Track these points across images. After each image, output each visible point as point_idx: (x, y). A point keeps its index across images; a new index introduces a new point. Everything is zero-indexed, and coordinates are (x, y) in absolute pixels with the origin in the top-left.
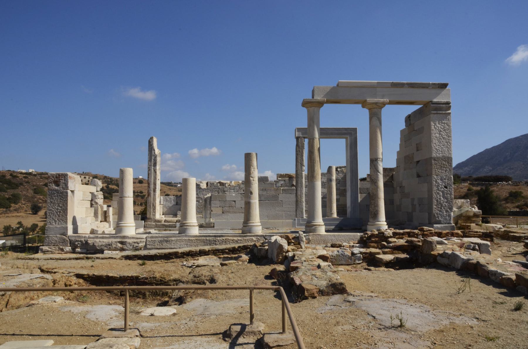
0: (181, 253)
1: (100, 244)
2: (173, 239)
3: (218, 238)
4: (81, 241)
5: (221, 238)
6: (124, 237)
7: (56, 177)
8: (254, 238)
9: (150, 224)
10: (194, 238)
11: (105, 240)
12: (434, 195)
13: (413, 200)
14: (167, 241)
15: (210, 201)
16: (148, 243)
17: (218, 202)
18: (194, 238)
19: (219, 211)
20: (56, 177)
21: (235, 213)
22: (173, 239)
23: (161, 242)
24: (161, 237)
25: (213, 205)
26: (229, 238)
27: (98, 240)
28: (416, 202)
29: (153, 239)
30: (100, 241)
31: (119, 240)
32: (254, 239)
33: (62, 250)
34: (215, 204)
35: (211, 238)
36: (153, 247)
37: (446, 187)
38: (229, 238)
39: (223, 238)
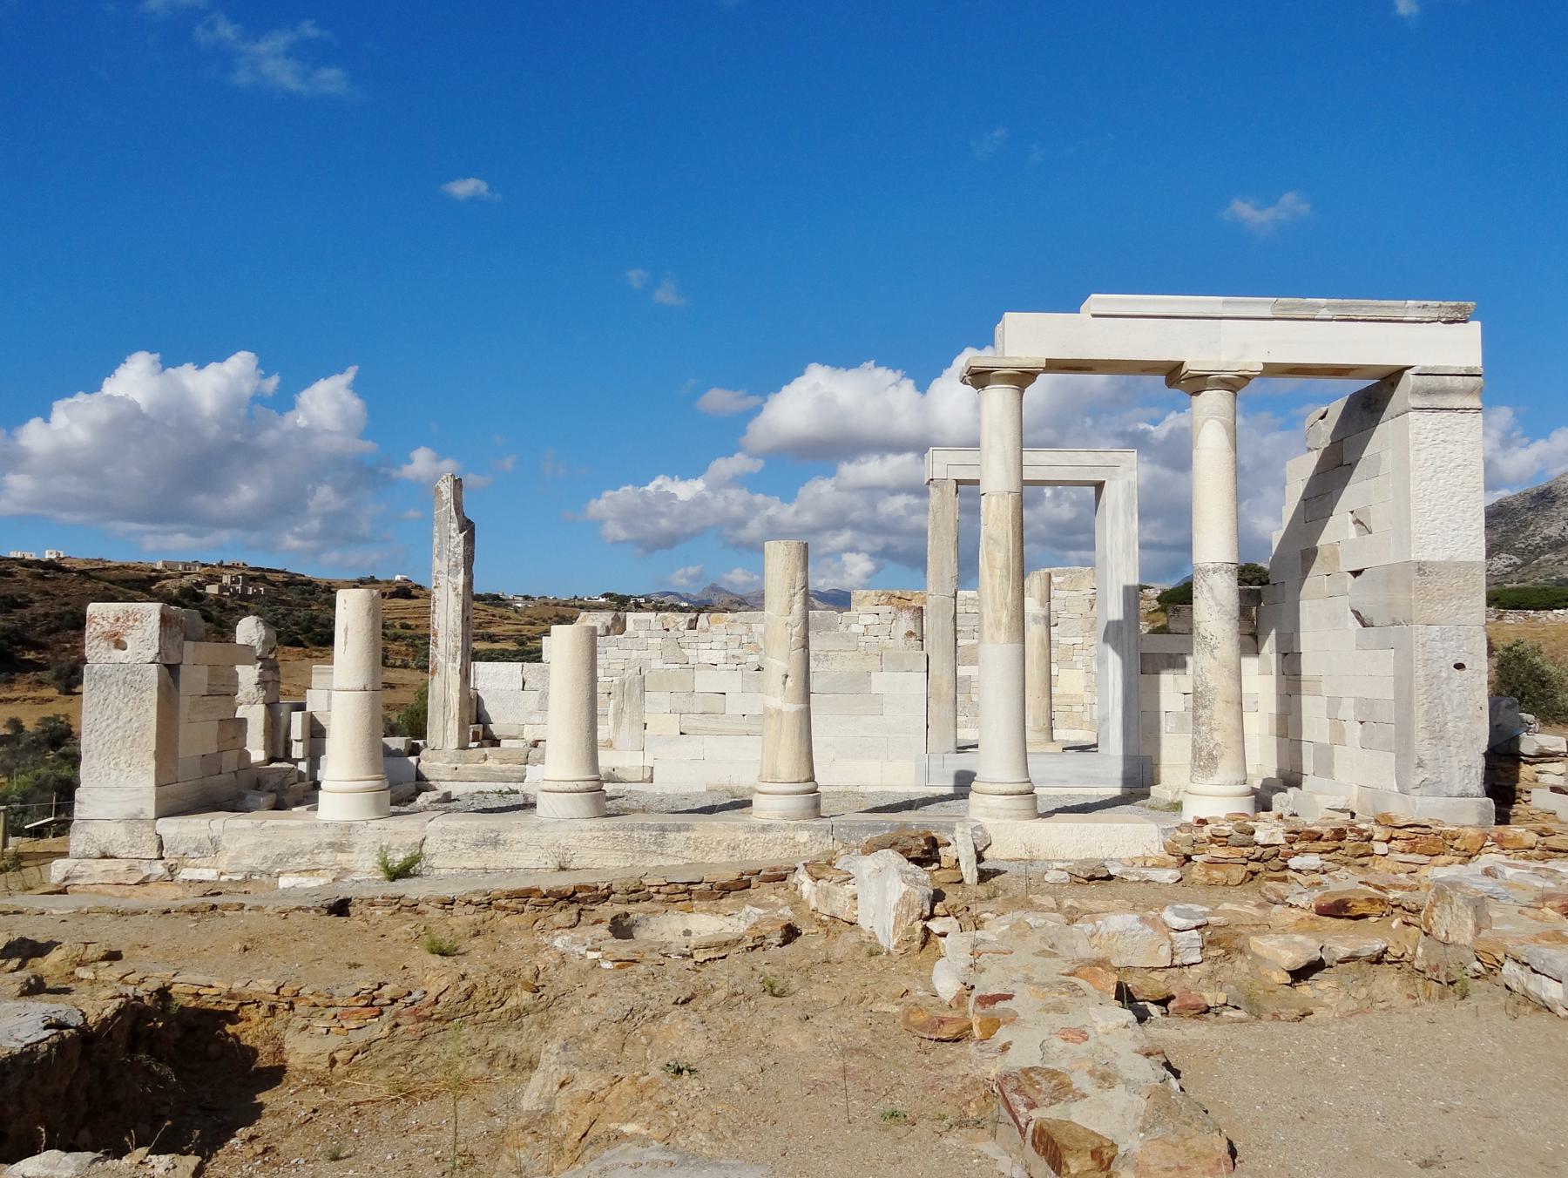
0: (550, 893)
2: (516, 836)
13: (1334, 703)
14: (495, 843)
19: (672, 725)
25: (648, 708)
28: (1348, 711)
37: (1459, 666)
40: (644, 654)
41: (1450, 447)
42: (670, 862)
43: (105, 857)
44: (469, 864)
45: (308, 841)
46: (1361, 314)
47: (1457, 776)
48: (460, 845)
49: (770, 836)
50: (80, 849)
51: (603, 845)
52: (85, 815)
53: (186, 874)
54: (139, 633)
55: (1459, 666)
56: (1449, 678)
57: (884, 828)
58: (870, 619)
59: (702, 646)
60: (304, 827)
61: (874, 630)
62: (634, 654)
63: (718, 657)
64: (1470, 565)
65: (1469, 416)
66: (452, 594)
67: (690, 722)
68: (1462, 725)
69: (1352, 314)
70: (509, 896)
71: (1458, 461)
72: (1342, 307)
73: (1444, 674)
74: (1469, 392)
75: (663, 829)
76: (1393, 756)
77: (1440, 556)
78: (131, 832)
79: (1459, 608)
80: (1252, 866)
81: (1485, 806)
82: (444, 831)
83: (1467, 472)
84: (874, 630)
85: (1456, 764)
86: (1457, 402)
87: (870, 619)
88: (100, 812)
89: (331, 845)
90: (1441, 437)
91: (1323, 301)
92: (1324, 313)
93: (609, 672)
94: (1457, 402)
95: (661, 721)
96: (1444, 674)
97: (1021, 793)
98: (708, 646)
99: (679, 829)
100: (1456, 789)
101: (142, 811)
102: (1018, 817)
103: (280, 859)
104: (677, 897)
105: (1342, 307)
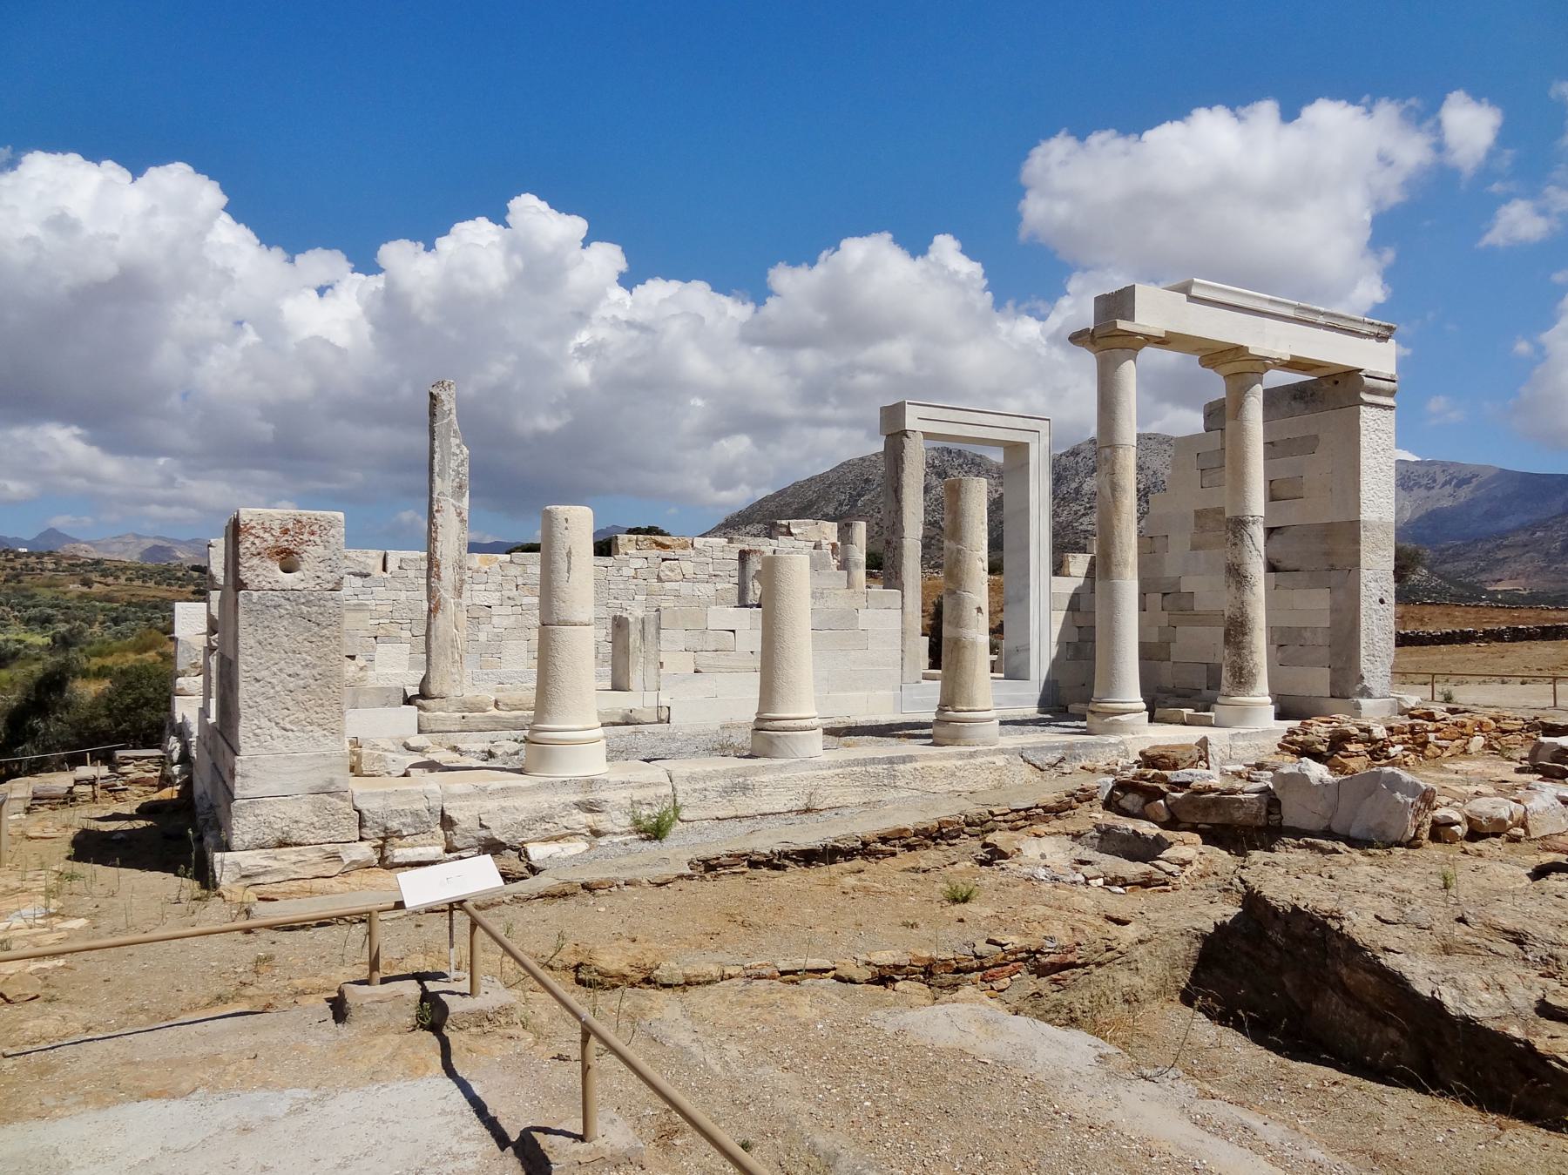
1: (507, 819)
2: (765, 778)
3: (902, 767)
4: (415, 814)
5: (909, 766)
6: (590, 783)
7: (286, 531)
8: (994, 759)
9: (443, 720)
10: (831, 772)
11: (522, 802)
12: (1363, 625)
14: (745, 788)
15: (659, 628)
16: (680, 800)
17: (679, 635)
18: (831, 772)
19: (685, 663)
20: (286, 531)
21: (732, 670)
22: (765, 778)
23: (727, 792)
24: (724, 775)
26: (934, 764)
27: (492, 804)
29: (700, 785)
30: (503, 809)
31: (576, 798)
32: (1000, 761)
33: (335, 857)
34: (673, 638)
35: (879, 768)
36: (703, 814)
38: (934, 764)
39: (915, 765)
42: (904, 794)
43: (282, 844)
44: (721, 814)
45: (544, 801)
48: (711, 795)
49: (979, 761)
50: (247, 838)
51: (845, 782)
52: (250, 793)
53: (400, 854)
54: (320, 550)
55: (1382, 601)
57: (1057, 748)
58: (639, 563)
59: (476, 587)
60: (540, 787)
61: (643, 573)
63: (493, 599)
66: (456, 520)
67: (705, 659)
70: (884, 840)
75: (891, 761)
76: (1327, 671)
78: (319, 810)
82: (691, 779)
84: (643, 573)
87: (639, 563)
88: (274, 788)
89: (578, 805)
93: (375, 614)
95: (677, 661)
98: (482, 587)
99: (905, 760)
101: (332, 782)
103: (525, 826)
104: (1020, 823)
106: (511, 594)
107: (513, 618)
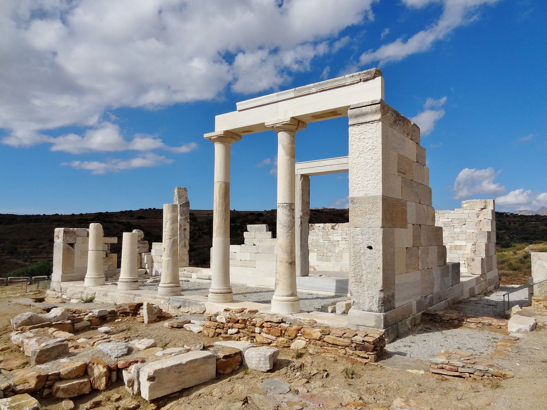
37: (370, 248)
40: (318, 238)
41: (367, 141)
46: (328, 86)
47: (367, 301)
55: (370, 248)
56: (364, 253)
62: (315, 238)
63: (339, 238)
64: (375, 198)
65: (375, 124)
68: (369, 276)
69: (324, 87)
71: (370, 147)
72: (319, 85)
73: (362, 251)
74: (375, 112)
77: (361, 194)
79: (370, 219)
80: (218, 331)
81: (378, 317)
83: (374, 152)
85: (366, 295)
86: (368, 119)
90: (363, 137)
91: (312, 85)
92: (314, 90)
94: (368, 119)
96: (362, 251)
97: (217, 293)
98: (336, 235)
100: (366, 307)
102: (214, 302)
105: (319, 85)
106: (346, 237)
107: (346, 245)
